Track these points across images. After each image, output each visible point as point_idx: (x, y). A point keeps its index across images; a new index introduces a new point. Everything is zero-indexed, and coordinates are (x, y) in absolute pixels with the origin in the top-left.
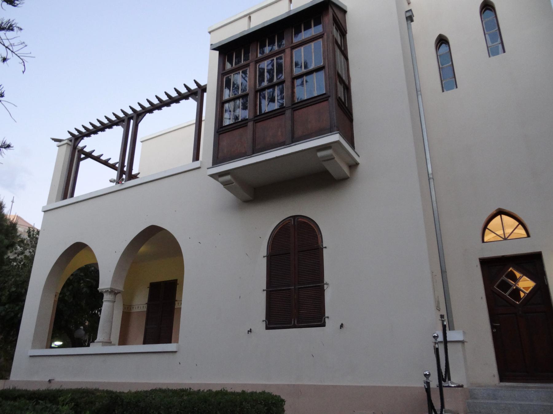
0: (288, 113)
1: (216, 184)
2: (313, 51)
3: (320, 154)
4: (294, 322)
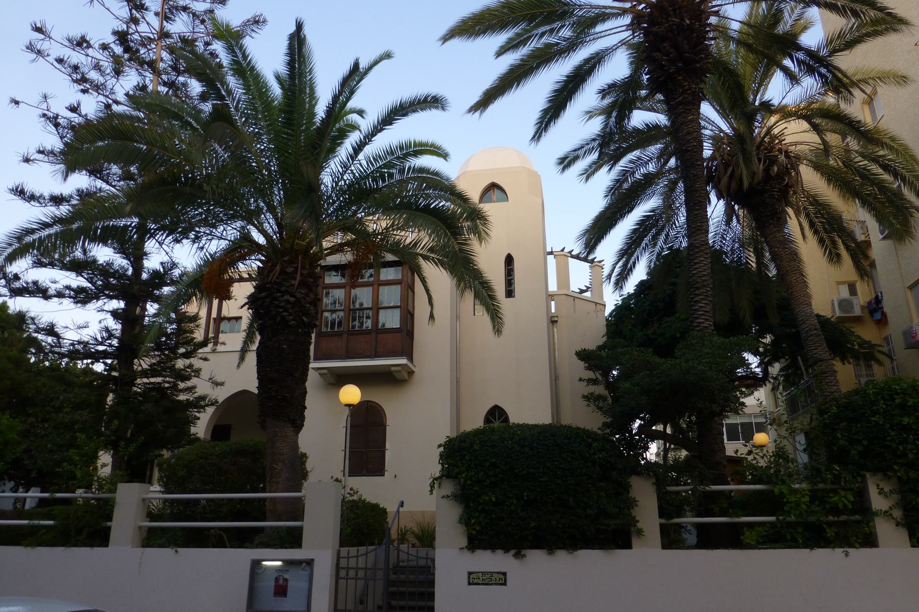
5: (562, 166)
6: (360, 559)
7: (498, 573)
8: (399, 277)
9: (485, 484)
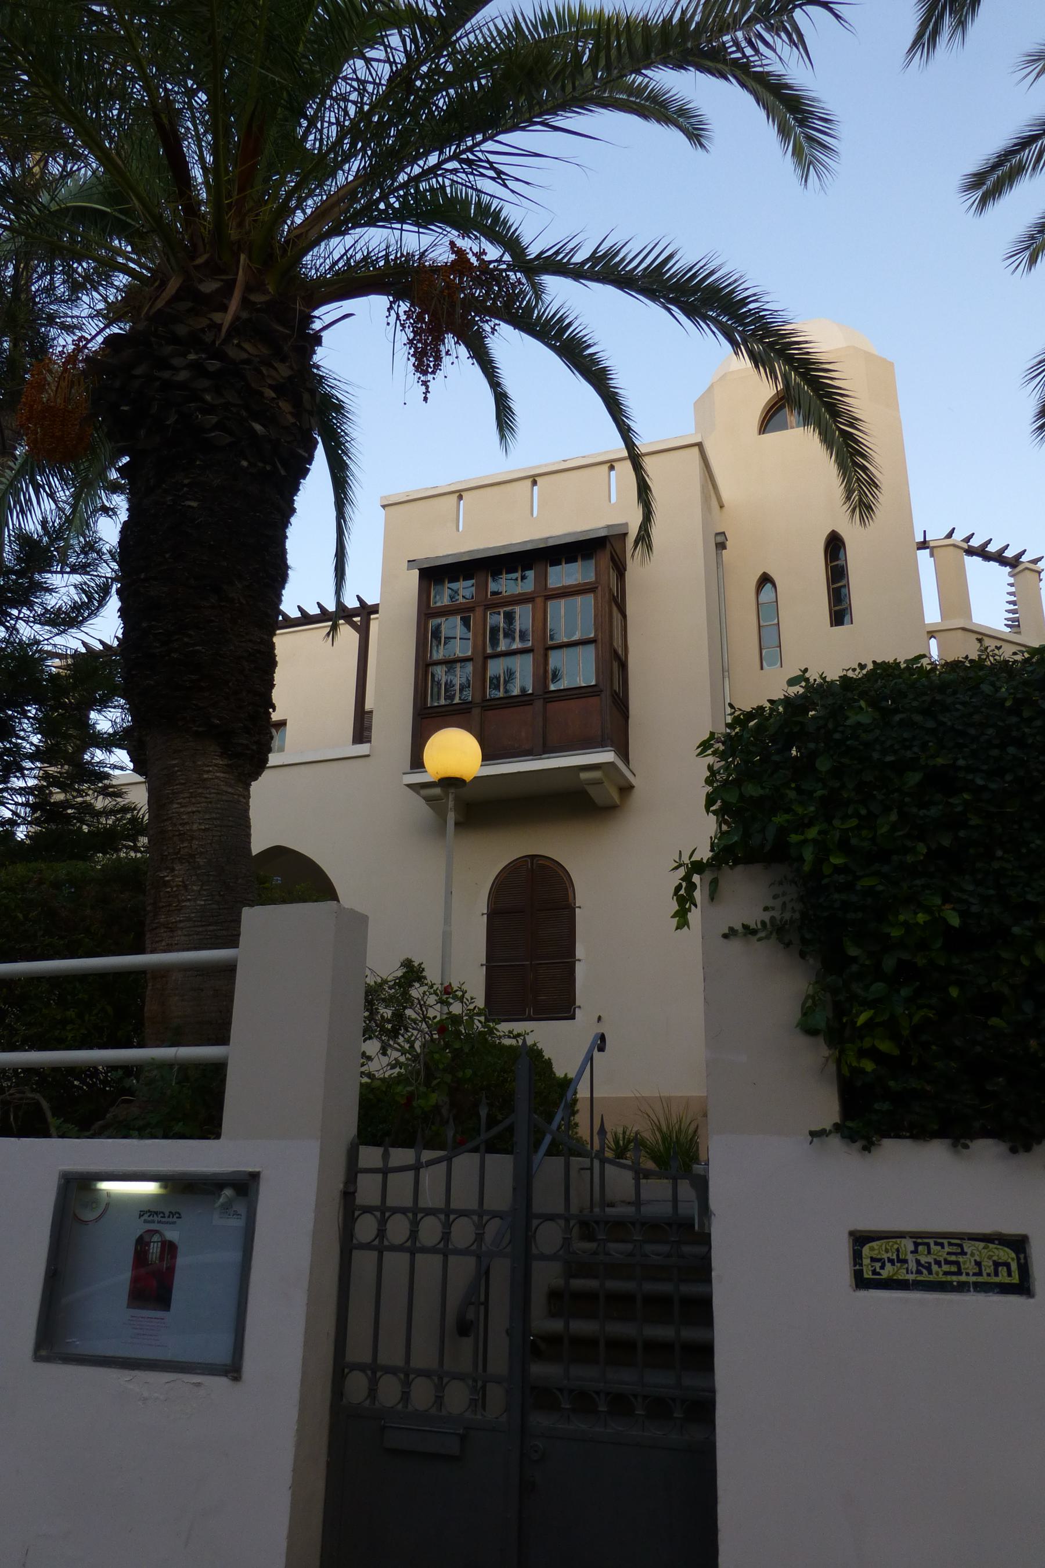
0: (539, 704)
1: (417, 802)
2: (579, 610)
3: (584, 776)
4: (530, 1011)
5: (979, 193)
6: (426, 1175)
7: (986, 1239)
8: (591, 577)
9: (909, 859)
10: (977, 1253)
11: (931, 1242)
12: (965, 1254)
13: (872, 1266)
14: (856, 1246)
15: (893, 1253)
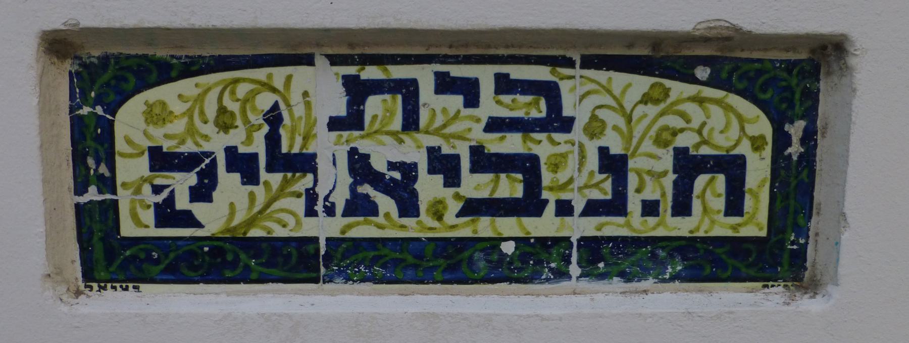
10: (611, 118)
11: (425, 76)
12: (567, 125)
13: (157, 190)
14: (85, 101)
15: (251, 129)
